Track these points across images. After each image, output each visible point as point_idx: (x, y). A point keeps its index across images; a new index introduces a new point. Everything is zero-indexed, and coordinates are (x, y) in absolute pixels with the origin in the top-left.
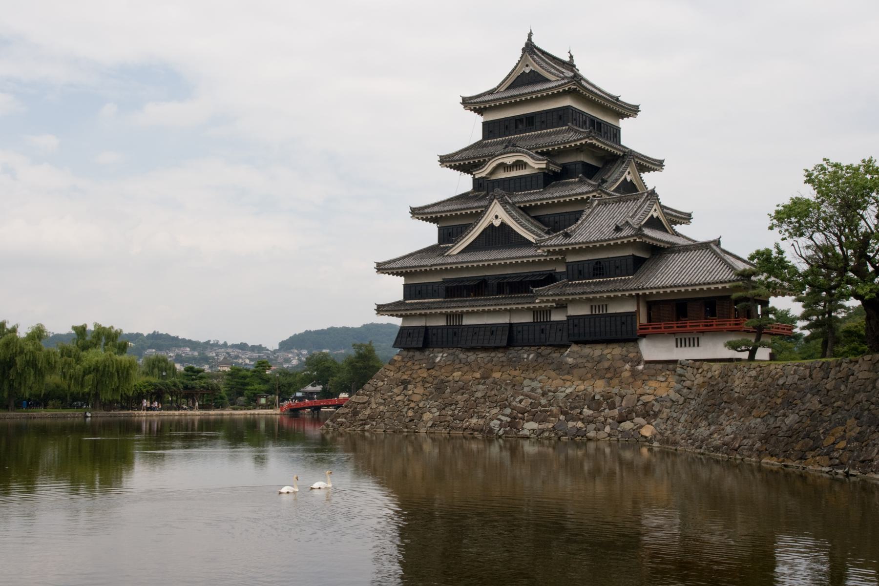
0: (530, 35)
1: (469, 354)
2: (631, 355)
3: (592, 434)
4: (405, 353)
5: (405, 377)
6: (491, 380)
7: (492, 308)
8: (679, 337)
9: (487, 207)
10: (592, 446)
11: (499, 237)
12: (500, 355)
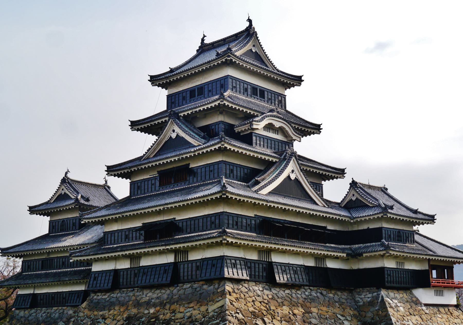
1: (278, 289)
2: (414, 299)
5: (251, 309)
12: (298, 292)
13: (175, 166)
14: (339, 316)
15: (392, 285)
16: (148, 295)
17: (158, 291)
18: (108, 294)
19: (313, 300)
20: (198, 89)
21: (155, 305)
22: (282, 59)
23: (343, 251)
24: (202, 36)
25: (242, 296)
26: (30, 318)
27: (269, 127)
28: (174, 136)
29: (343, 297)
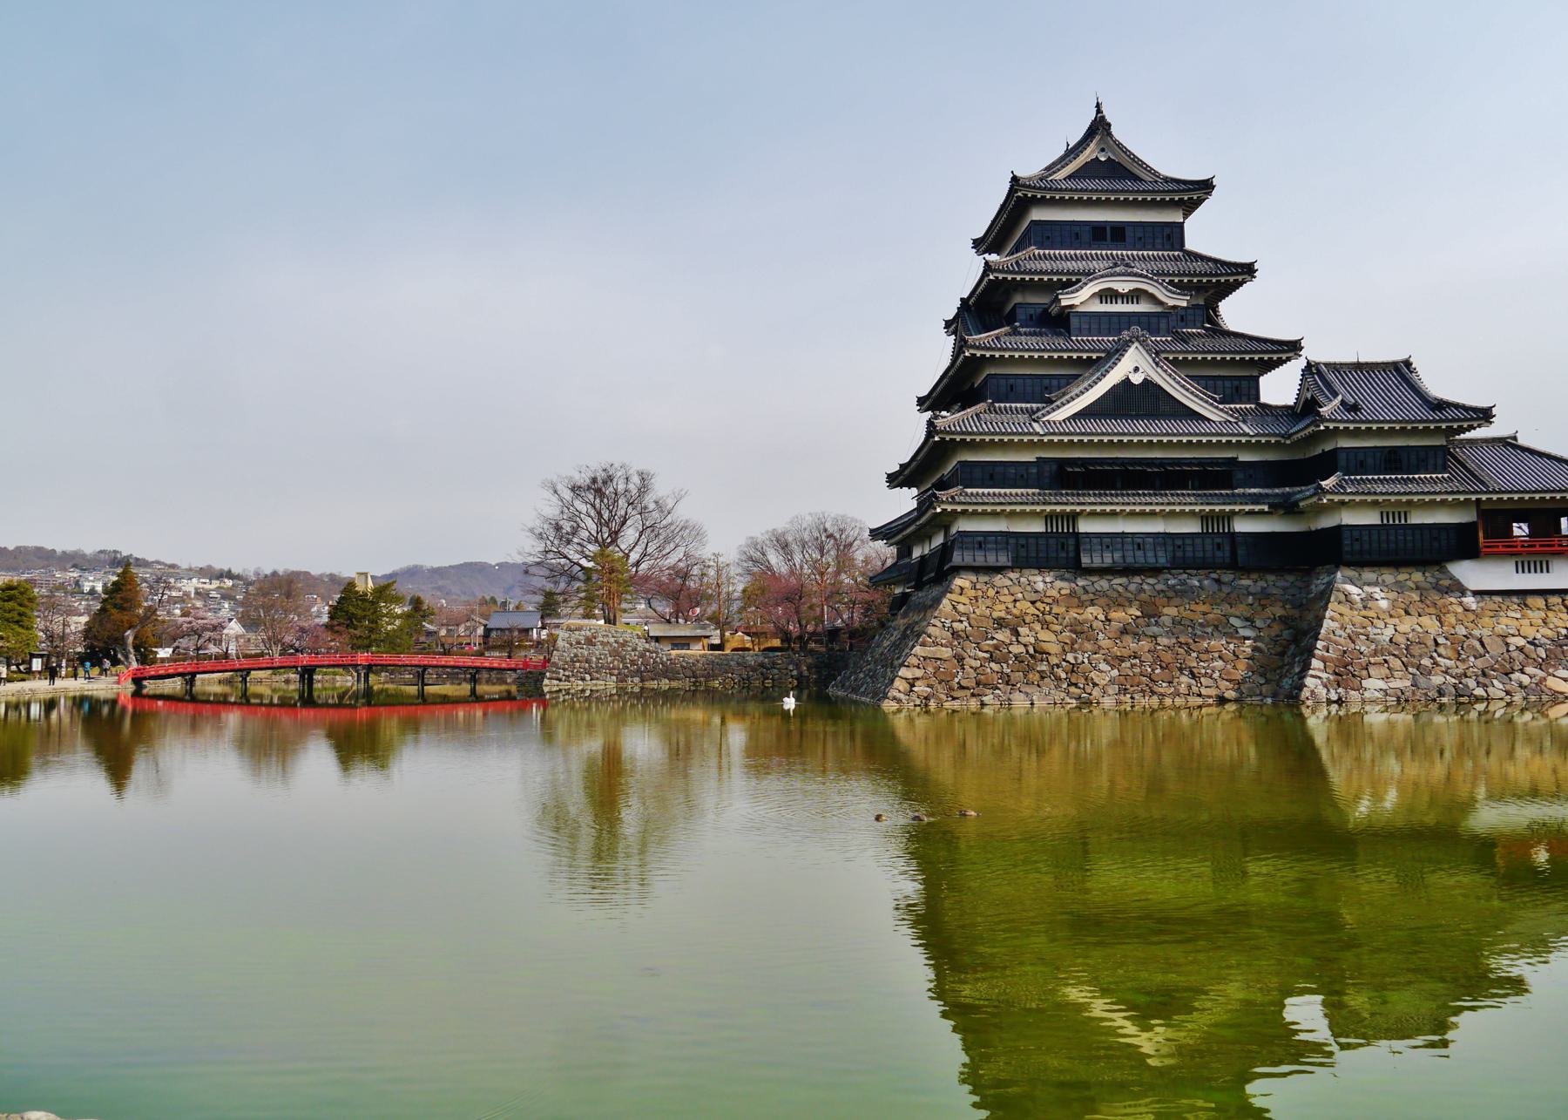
0: (1098, 105)
2: (1446, 583)
3: (1479, 692)
4: (974, 578)
5: (1003, 614)
6: (1166, 620)
7: (1138, 509)
8: (1519, 559)
9: (1116, 353)
10: (1480, 707)
11: (1134, 401)
12: (1151, 581)
14: (1233, 621)
15: (1367, 557)
19: (1183, 593)
22: (1169, 159)
23: (1256, 499)
25: (991, 593)
27: (1108, 295)
29: (1281, 583)
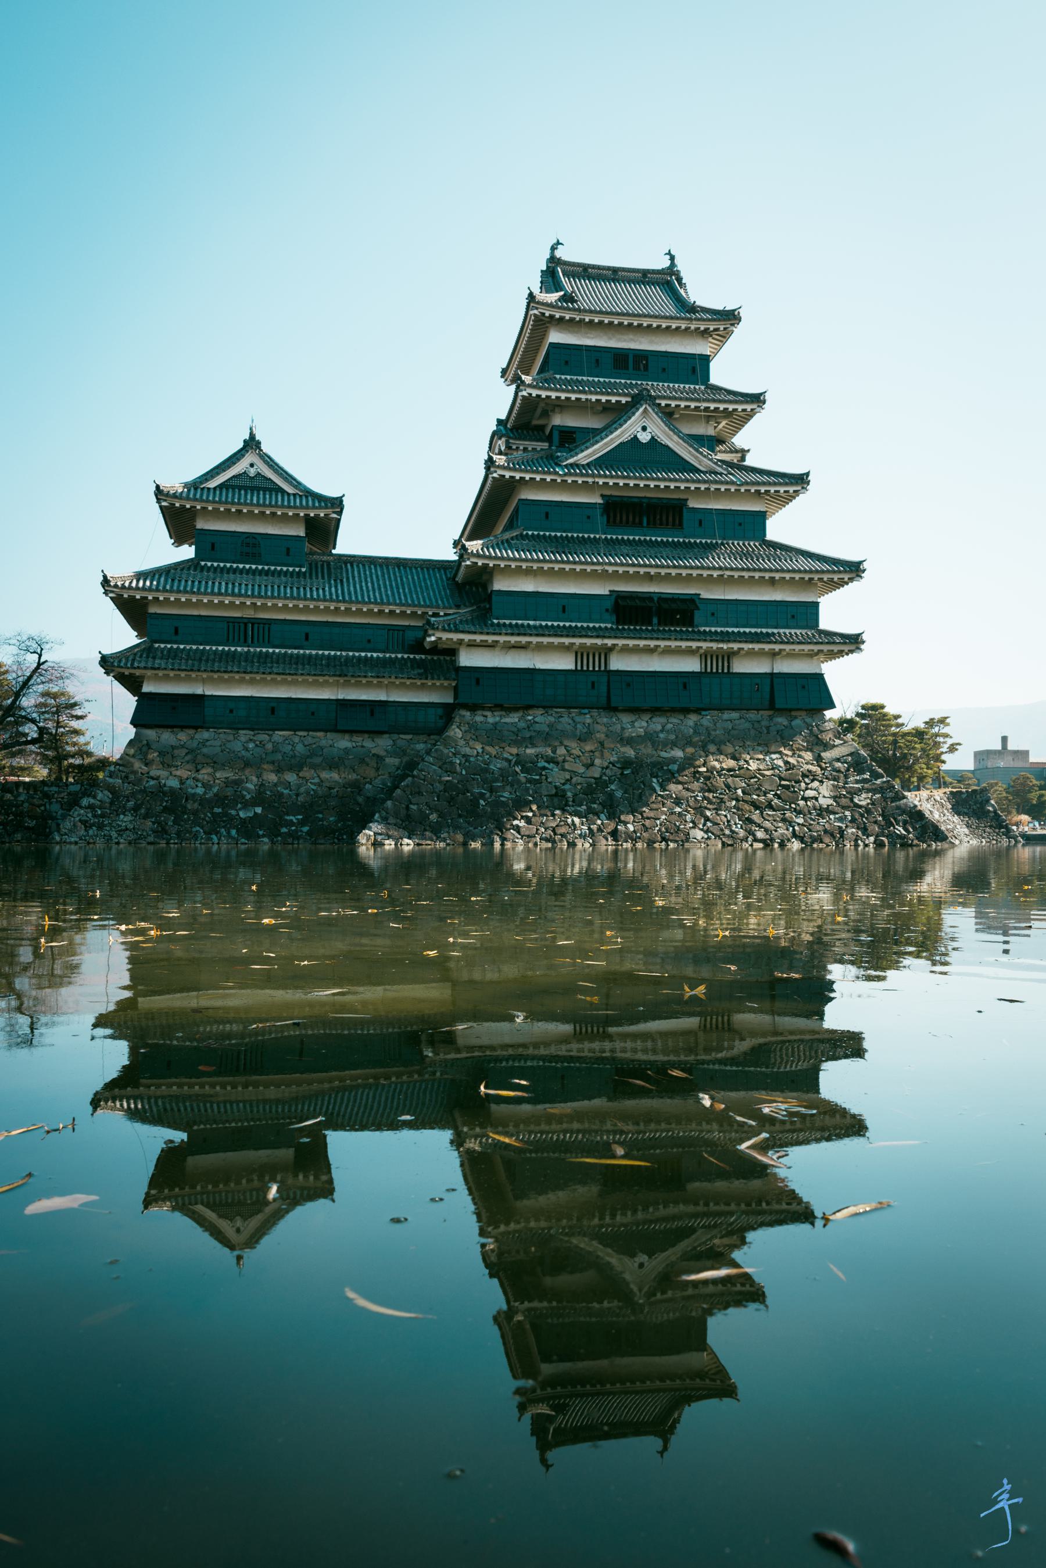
13: (649, 495)
16: (636, 724)
17: (663, 720)
18: (520, 714)
20: (635, 356)
21: (674, 744)
24: (555, 241)
26: (205, 750)
28: (644, 437)
